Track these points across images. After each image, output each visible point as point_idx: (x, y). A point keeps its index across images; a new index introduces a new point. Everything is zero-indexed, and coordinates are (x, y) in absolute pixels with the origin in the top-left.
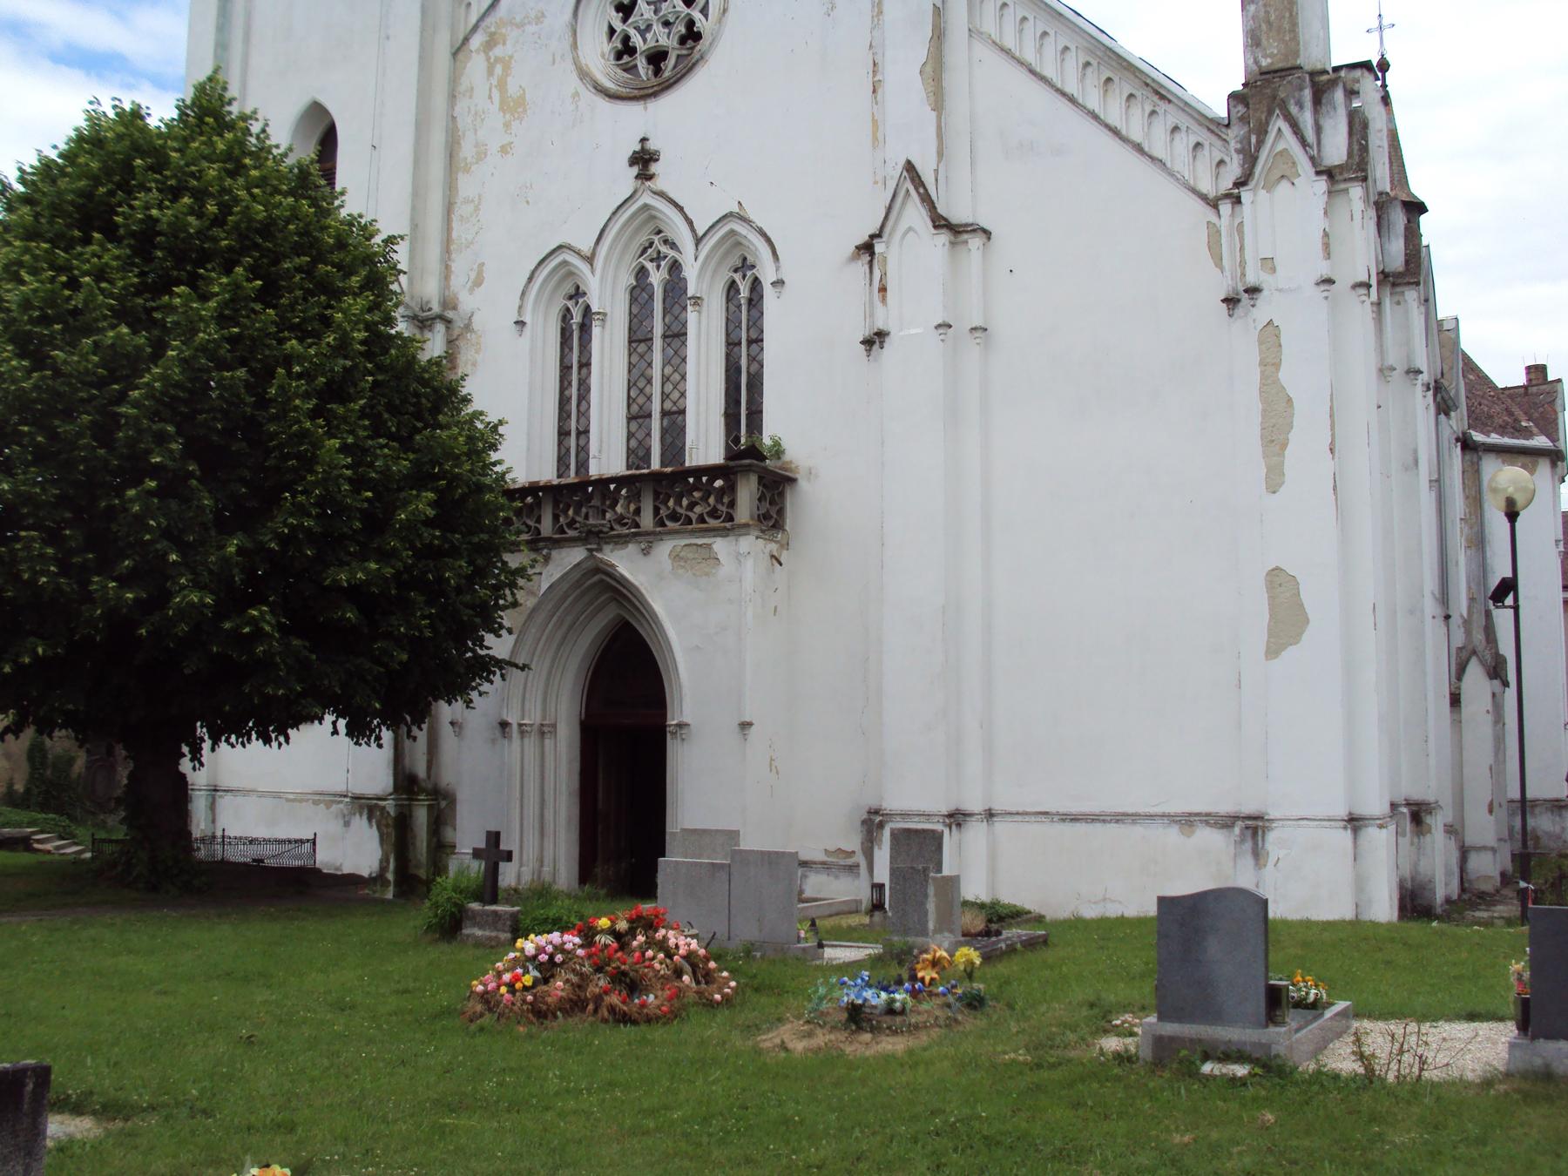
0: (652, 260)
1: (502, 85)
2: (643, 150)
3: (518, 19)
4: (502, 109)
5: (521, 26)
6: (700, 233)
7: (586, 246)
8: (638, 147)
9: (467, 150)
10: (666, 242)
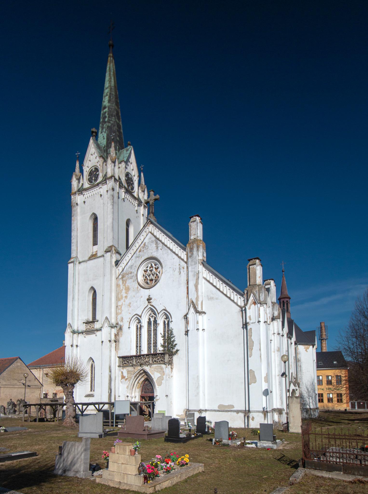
0: (151, 317)
1: (125, 285)
2: (149, 298)
3: (128, 273)
4: (125, 289)
5: (127, 274)
6: (159, 312)
7: (140, 314)
8: (148, 297)
9: (120, 296)
10: (153, 314)
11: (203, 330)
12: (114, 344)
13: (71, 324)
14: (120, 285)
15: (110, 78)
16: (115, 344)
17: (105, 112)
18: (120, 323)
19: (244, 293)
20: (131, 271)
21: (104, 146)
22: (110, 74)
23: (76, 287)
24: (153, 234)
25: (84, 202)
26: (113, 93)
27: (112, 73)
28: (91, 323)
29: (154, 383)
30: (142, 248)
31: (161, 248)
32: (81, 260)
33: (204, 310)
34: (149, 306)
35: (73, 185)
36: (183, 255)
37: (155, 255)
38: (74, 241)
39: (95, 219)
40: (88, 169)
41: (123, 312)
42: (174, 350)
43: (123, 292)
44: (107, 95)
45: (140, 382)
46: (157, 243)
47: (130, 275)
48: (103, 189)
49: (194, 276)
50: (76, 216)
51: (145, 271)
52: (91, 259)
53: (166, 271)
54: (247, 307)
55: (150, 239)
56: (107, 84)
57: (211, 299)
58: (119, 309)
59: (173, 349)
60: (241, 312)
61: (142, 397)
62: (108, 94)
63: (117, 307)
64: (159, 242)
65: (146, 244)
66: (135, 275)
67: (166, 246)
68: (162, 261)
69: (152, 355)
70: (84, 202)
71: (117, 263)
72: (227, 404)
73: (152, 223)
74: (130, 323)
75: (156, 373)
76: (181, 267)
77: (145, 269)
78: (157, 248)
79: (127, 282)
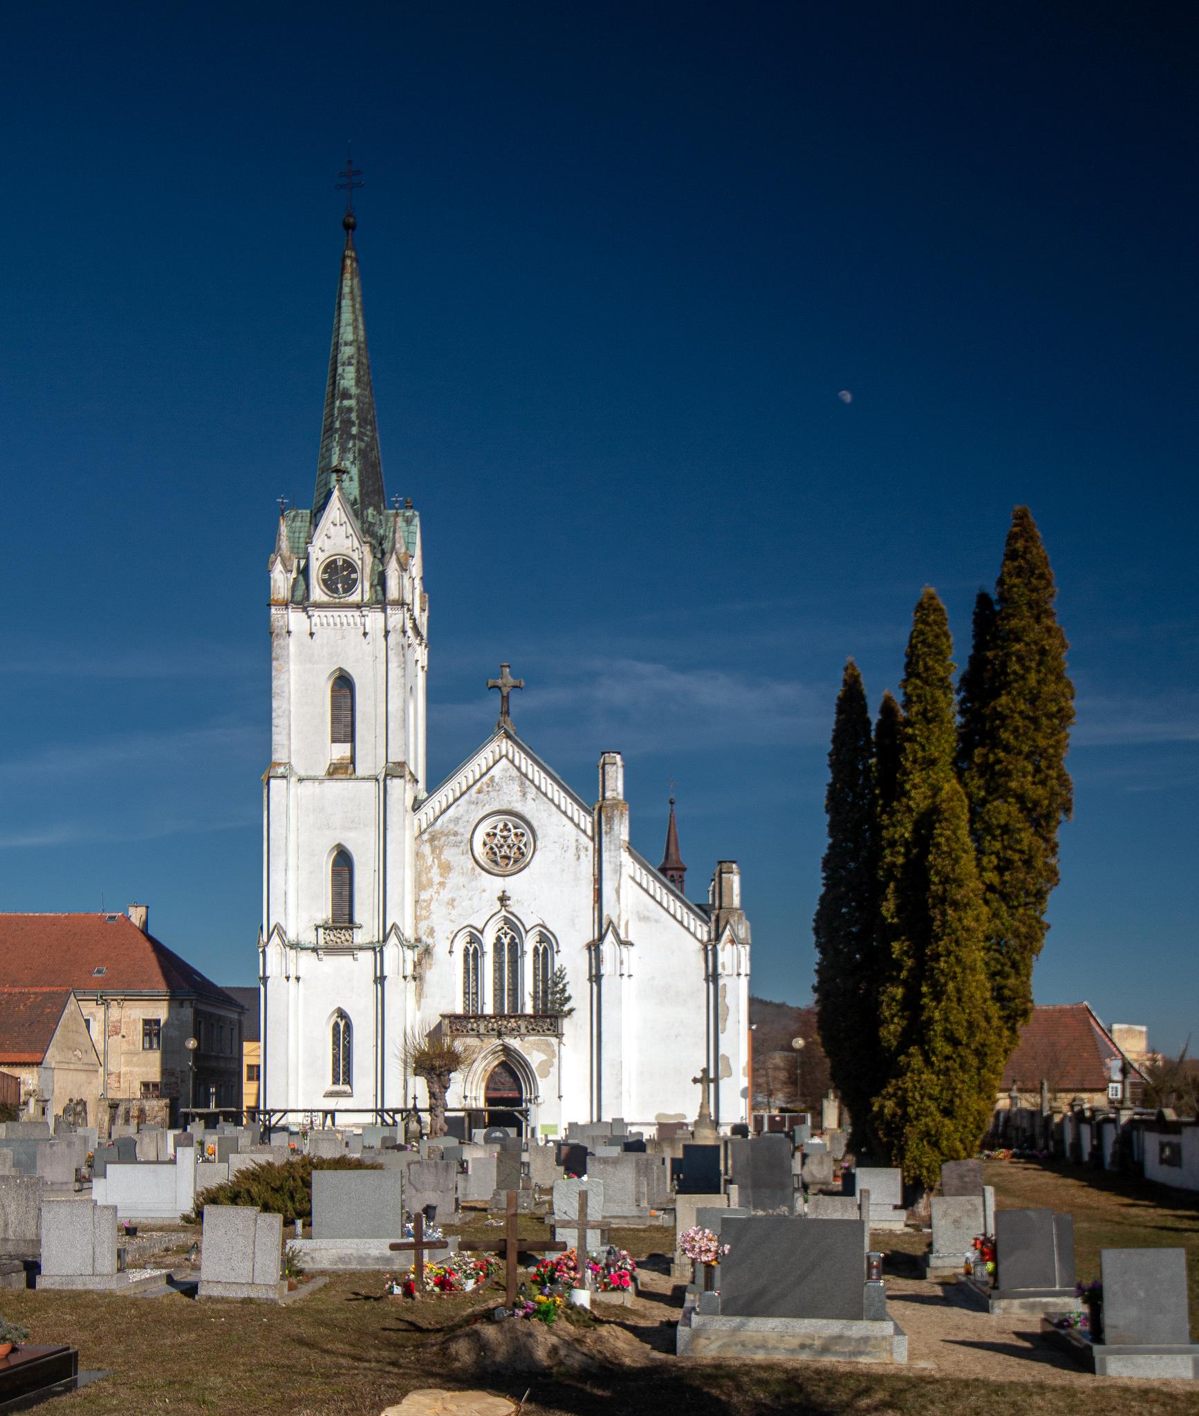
1: (439, 858)
4: (439, 867)
5: (446, 835)
7: (480, 927)
9: (424, 879)
11: (621, 975)
12: (412, 985)
13: (283, 925)
14: (424, 856)
15: (356, 320)
16: (413, 983)
17: (350, 410)
18: (424, 938)
19: (710, 918)
20: (456, 829)
21: (352, 498)
22: (353, 306)
23: (292, 838)
24: (512, 762)
25: (312, 634)
26: (364, 361)
27: (358, 306)
28: (341, 929)
29: (531, 1071)
30: (485, 787)
31: (533, 796)
32: (302, 773)
33: (630, 938)
34: (503, 913)
35: (275, 581)
36: (586, 822)
37: (518, 807)
38: (278, 721)
39: (343, 684)
40: (322, 556)
41: (433, 916)
42: (566, 1008)
43: (433, 871)
44: (350, 364)
45: (490, 1069)
46: (522, 784)
47: (452, 838)
48: (374, 620)
49: (615, 871)
50: (288, 663)
51: (488, 835)
52: (335, 777)
53: (545, 847)
54: (719, 947)
55: (506, 770)
56: (347, 334)
57: (644, 918)
58: (421, 909)
59: (562, 1005)
60: (702, 954)
61: (490, 1101)
62: (354, 361)
63: (417, 902)
64: (528, 783)
65: (496, 780)
66: (466, 841)
67: (545, 795)
68: (535, 824)
69: (541, 1017)
70: (312, 634)
71: (417, 806)
72: (672, 1113)
73: (509, 737)
74: (452, 942)
75: (535, 1053)
76: (581, 846)
77: (488, 830)
78: (524, 795)
79: (445, 852)
